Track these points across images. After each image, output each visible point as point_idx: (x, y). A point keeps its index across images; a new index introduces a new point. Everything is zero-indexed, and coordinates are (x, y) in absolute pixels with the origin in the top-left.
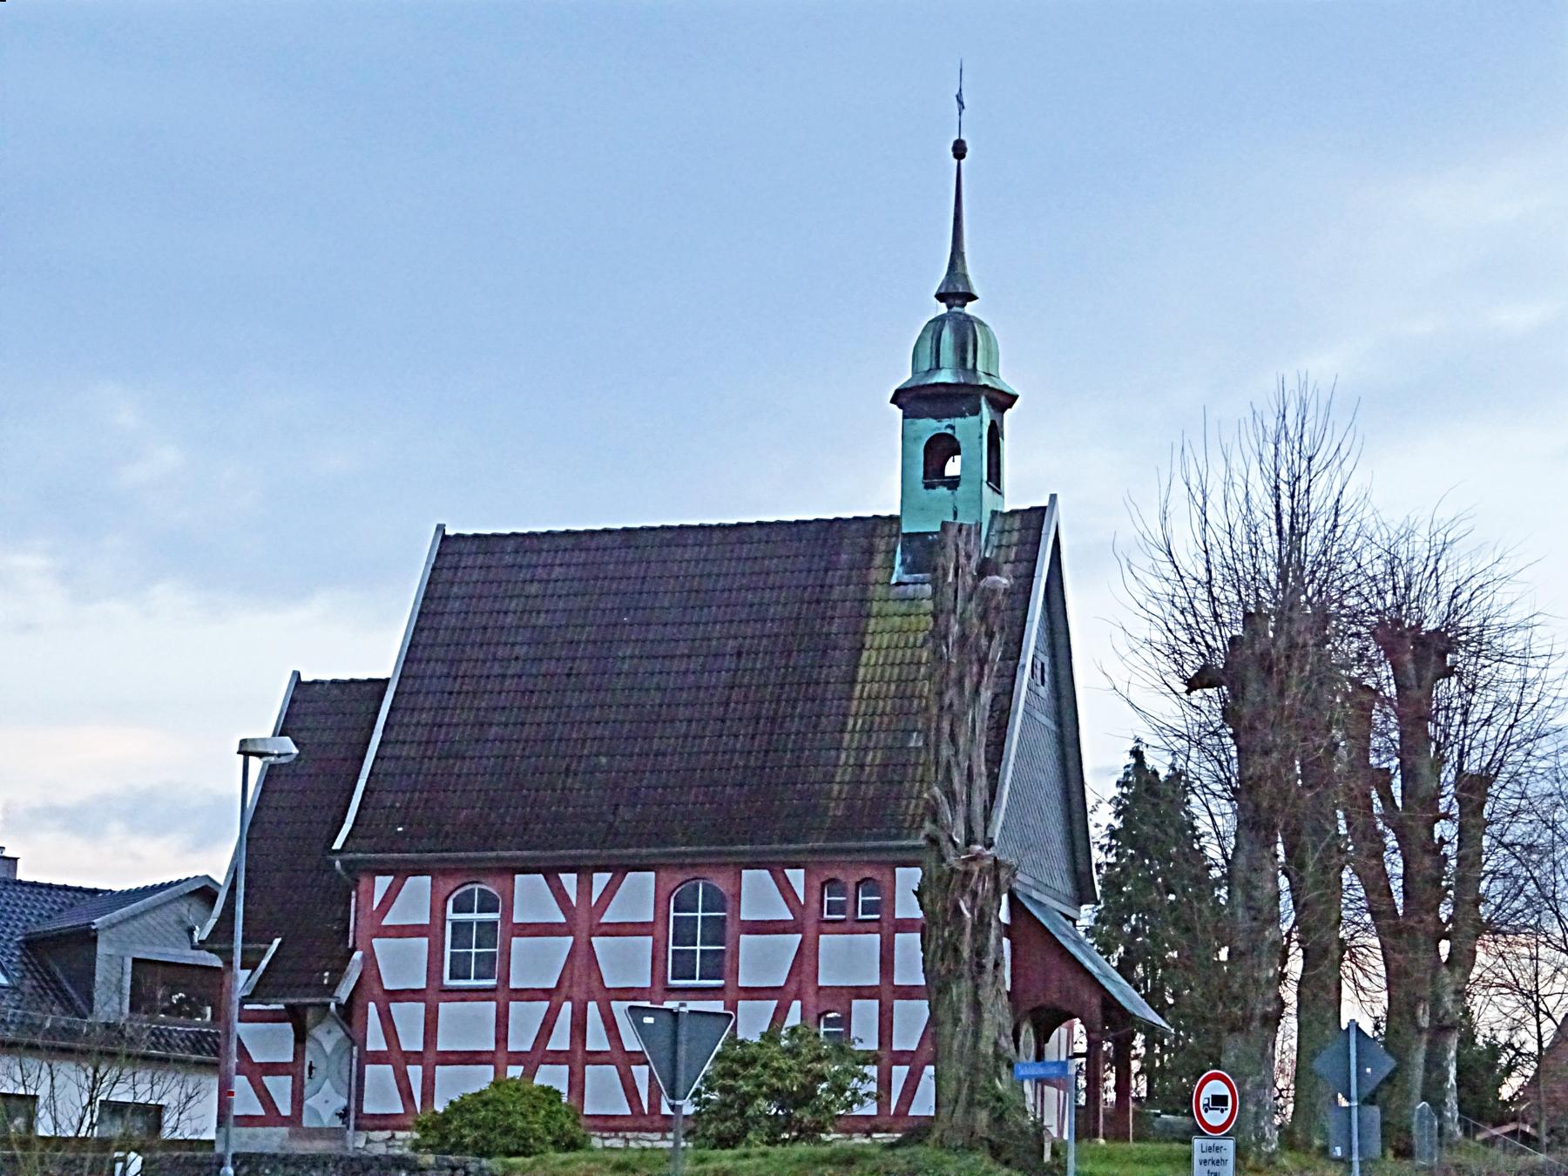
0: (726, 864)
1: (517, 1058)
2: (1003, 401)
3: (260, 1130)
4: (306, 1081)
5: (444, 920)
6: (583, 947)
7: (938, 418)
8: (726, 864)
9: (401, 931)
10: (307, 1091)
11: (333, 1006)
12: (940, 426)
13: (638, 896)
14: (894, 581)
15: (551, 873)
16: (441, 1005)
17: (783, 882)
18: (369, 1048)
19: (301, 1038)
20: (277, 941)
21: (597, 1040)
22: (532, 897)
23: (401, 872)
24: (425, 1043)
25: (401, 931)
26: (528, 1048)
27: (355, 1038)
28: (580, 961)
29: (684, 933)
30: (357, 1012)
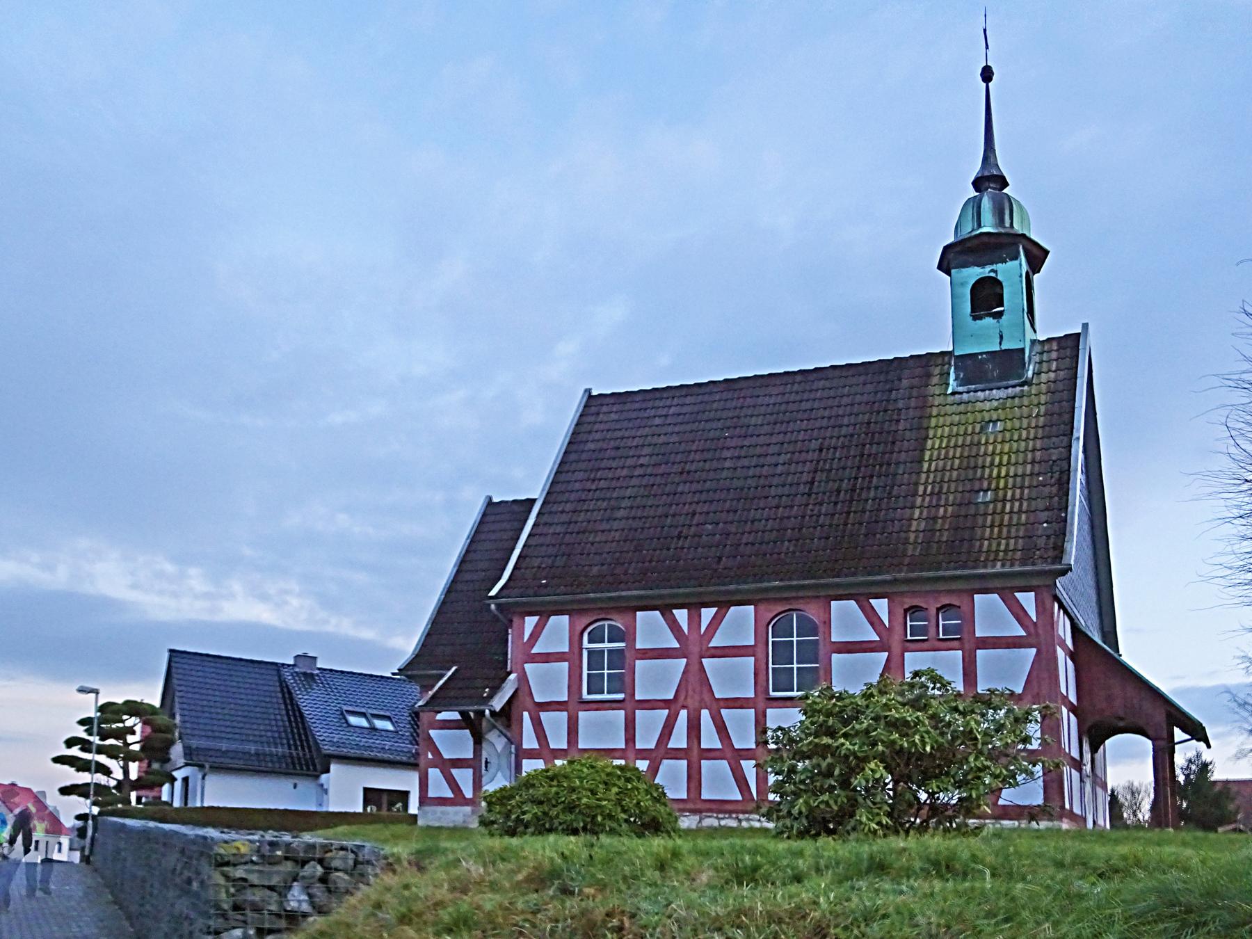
0: (818, 597)
1: (643, 754)
2: (1037, 257)
3: (450, 809)
4: (483, 771)
5: (581, 649)
6: (695, 668)
7: (982, 265)
8: (818, 597)
9: (546, 658)
10: (484, 780)
11: (487, 712)
12: (986, 271)
13: (741, 624)
14: (950, 391)
15: (666, 610)
16: (581, 714)
17: (868, 608)
18: (525, 746)
19: (478, 740)
20: (454, 669)
21: (710, 739)
22: (650, 628)
23: (544, 613)
24: (569, 742)
25: (546, 658)
26: (653, 746)
27: (515, 740)
28: (693, 679)
29: (783, 652)
30: (514, 717)
